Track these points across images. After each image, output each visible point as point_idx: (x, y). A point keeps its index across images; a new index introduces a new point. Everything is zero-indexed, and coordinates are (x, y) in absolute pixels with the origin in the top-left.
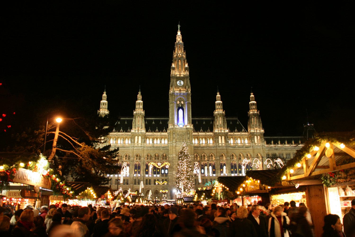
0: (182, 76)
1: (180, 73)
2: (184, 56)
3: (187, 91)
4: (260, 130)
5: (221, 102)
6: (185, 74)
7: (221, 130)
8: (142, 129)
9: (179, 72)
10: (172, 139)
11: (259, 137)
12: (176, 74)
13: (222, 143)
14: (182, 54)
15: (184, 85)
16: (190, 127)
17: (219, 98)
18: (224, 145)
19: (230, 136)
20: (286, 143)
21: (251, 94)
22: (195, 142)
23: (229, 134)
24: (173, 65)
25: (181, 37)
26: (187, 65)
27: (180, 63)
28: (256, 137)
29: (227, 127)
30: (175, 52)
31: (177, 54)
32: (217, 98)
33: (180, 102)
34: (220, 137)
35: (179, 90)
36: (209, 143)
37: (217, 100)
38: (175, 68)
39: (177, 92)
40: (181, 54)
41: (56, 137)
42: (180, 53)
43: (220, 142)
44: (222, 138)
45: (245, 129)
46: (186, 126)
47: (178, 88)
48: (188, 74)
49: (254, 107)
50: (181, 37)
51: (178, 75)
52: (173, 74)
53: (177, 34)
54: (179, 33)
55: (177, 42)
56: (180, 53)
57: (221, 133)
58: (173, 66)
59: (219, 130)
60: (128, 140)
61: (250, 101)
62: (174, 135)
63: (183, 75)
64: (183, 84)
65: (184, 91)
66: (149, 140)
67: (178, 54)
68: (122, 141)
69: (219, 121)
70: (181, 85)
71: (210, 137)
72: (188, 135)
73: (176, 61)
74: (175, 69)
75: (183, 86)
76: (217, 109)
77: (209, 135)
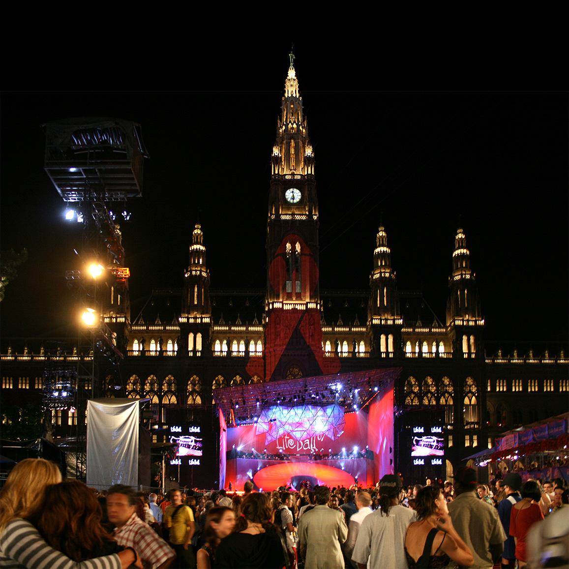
0: (299, 177)
1: (293, 171)
2: (304, 131)
3: (310, 216)
4: (476, 321)
5: (388, 250)
6: (306, 173)
10: (273, 336)
11: (472, 338)
12: (285, 173)
13: (387, 353)
15: (301, 200)
16: (317, 306)
17: (383, 240)
18: (391, 355)
19: (405, 336)
20: (515, 354)
21: (458, 231)
24: (276, 151)
25: (296, 84)
28: (465, 338)
29: (399, 313)
32: (380, 241)
34: (383, 337)
35: (291, 213)
36: (339, 350)
37: (378, 244)
38: (281, 157)
40: (295, 126)
43: (383, 349)
44: (389, 340)
45: (439, 321)
46: (307, 304)
50: (296, 82)
51: (288, 175)
52: (276, 172)
54: (292, 73)
55: (286, 95)
57: (386, 326)
58: (276, 154)
59: (381, 320)
61: (455, 250)
62: (278, 326)
64: (300, 197)
65: (303, 215)
67: (288, 124)
69: (382, 298)
70: (295, 201)
72: (312, 327)
73: (284, 142)
74: (281, 161)
75: (300, 205)
76: (378, 267)
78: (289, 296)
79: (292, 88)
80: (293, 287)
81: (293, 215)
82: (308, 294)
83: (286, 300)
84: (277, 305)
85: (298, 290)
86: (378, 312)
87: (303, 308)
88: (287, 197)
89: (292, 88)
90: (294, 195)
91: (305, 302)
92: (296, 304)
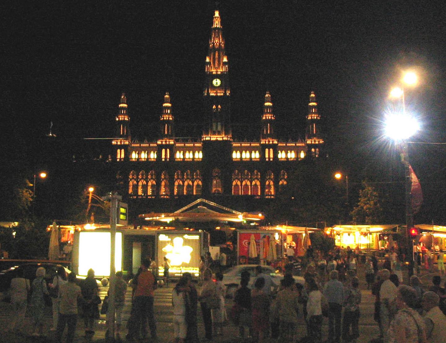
0: (220, 73)
2: (223, 45)
3: (225, 93)
7: (269, 141)
8: (170, 141)
9: (216, 68)
12: (212, 71)
13: (269, 158)
14: (220, 44)
18: (271, 160)
22: (236, 155)
23: (279, 145)
24: (208, 60)
25: (219, 20)
26: (225, 60)
27: (217, 56)
30: (211, 41)
31: (214, 44)
33: (217, 107)
34: (267, 150)
35: (215, 92)
39: (212, 94)
40: (218, 44)
41: (90, 198)
42: (217, 41)
43: (267, 156)
46: (223, 137)
47: (214, 90)
48: (227, 71)
49: (314, 111)
53: (214, 14)
54: (217, 14)
56: (217, 41)
60: (154, 153)
63: (221, 72)
64: (220, 83)
66: (180, 152)
68: (146, 154)
70: (218, 85)
71: (255, 149)
75: (220, 87)
77: (254, 147)
78: (214, 133)
79: (217, 24)
80: (217, 128)
81: (216, 93)
82: (224, 133)
83: (213, 135)
84: (208, 139)
85: (219, 128)
86: (265, 137)
87: (221, 139)
88: (213, 83)
89: (217, 24)
90: (217, 82)
91: (221, 136)
92: (217, 138)
